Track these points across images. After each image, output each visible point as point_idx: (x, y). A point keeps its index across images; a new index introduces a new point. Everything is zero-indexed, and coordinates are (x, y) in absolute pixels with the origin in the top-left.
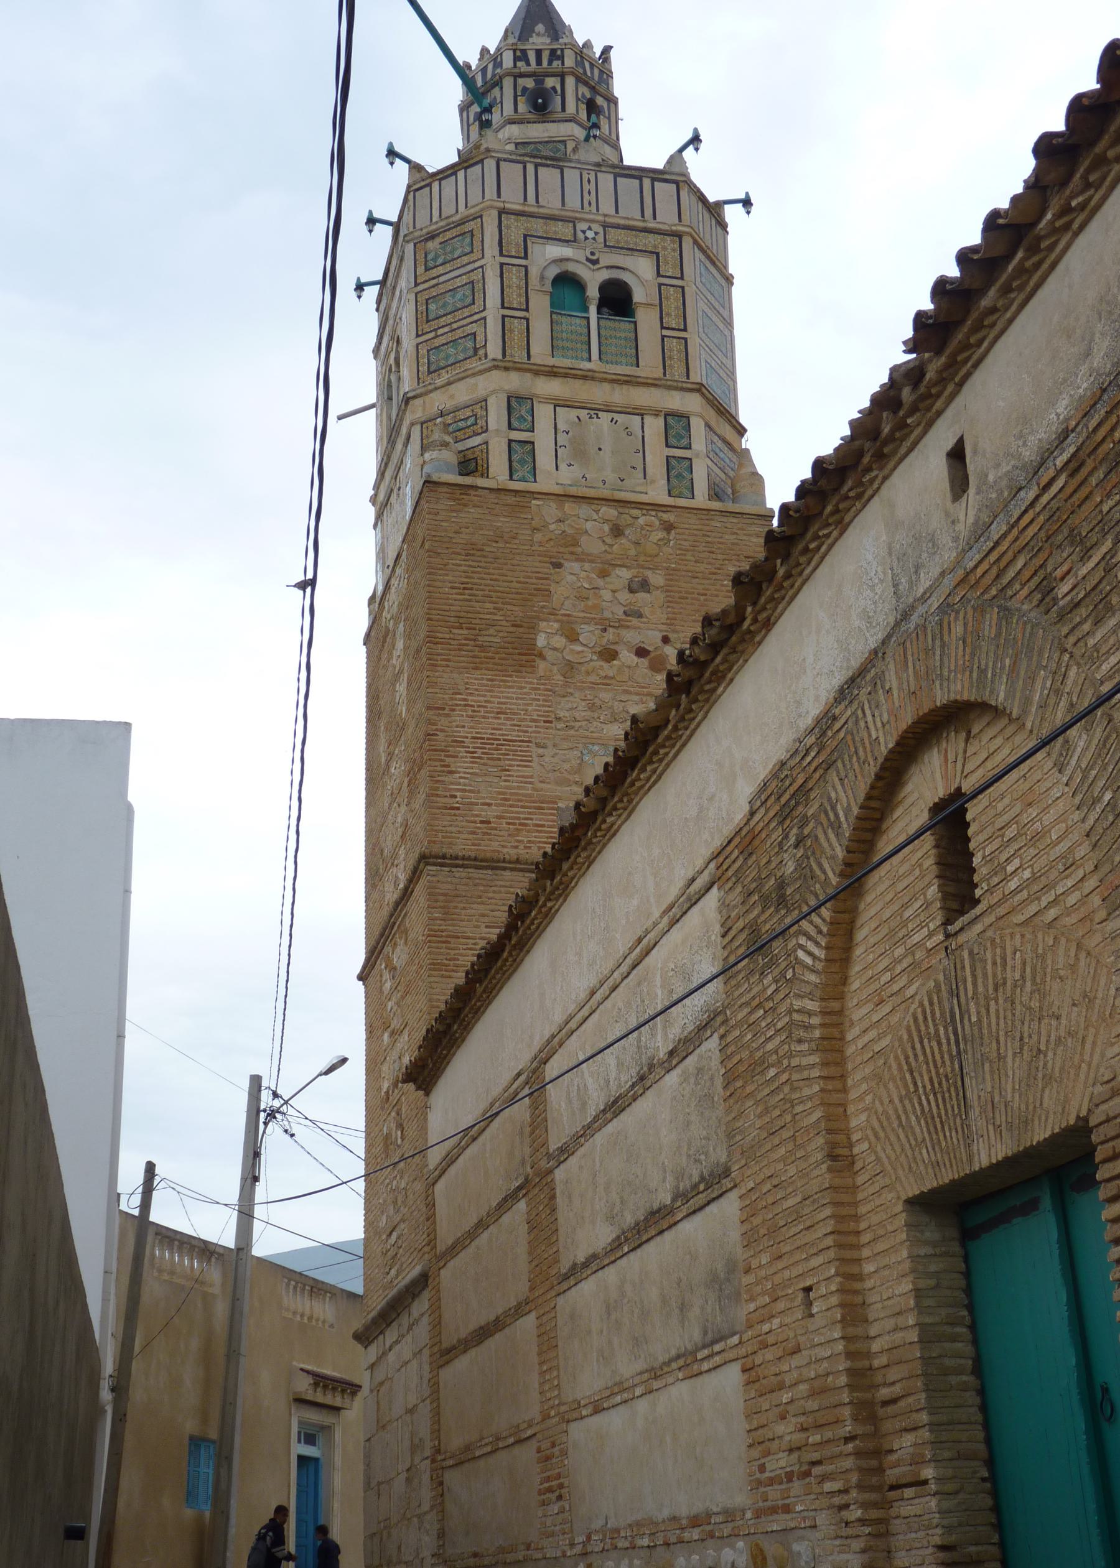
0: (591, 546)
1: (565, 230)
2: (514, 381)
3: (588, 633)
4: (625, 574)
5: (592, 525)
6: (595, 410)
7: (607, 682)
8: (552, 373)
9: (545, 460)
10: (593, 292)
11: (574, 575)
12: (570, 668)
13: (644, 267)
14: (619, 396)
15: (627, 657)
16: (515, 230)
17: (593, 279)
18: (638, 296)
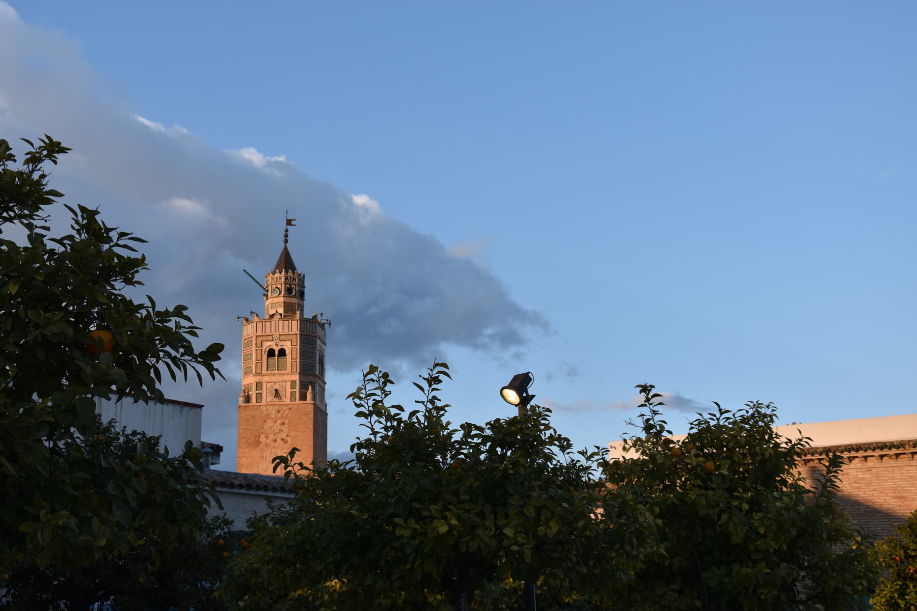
0: (273, 416)
1: (270, 338)
2: (258, 379)
3: (271, 437)
4: (279, 422)
5: (273, 411)
6: (275, 383)
7: (274, 447)
8: (266, 375)
9: (264, 397)
10: (277, 353)
11: (269, 423)
12: (267, 445)
13: (289, 343)
14: (281, 378)
15: (279, 441)
16: (259, 339)
17: (277, 349)
18: (287, 352)
